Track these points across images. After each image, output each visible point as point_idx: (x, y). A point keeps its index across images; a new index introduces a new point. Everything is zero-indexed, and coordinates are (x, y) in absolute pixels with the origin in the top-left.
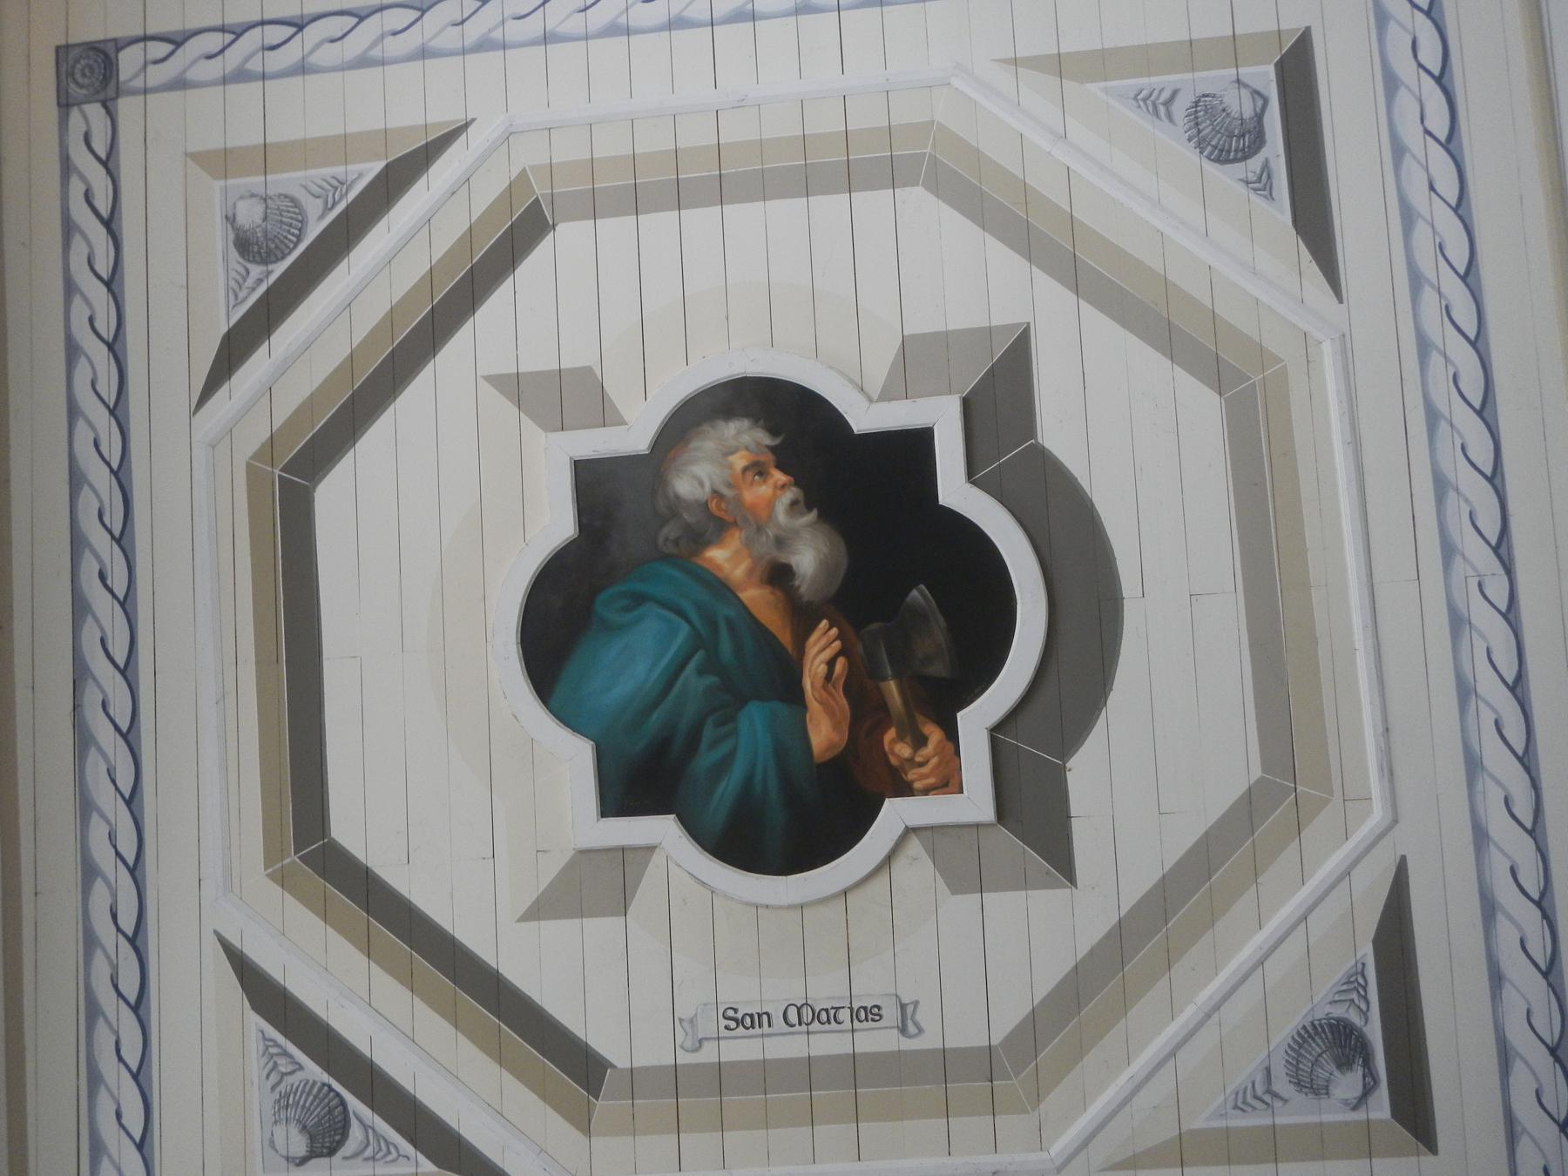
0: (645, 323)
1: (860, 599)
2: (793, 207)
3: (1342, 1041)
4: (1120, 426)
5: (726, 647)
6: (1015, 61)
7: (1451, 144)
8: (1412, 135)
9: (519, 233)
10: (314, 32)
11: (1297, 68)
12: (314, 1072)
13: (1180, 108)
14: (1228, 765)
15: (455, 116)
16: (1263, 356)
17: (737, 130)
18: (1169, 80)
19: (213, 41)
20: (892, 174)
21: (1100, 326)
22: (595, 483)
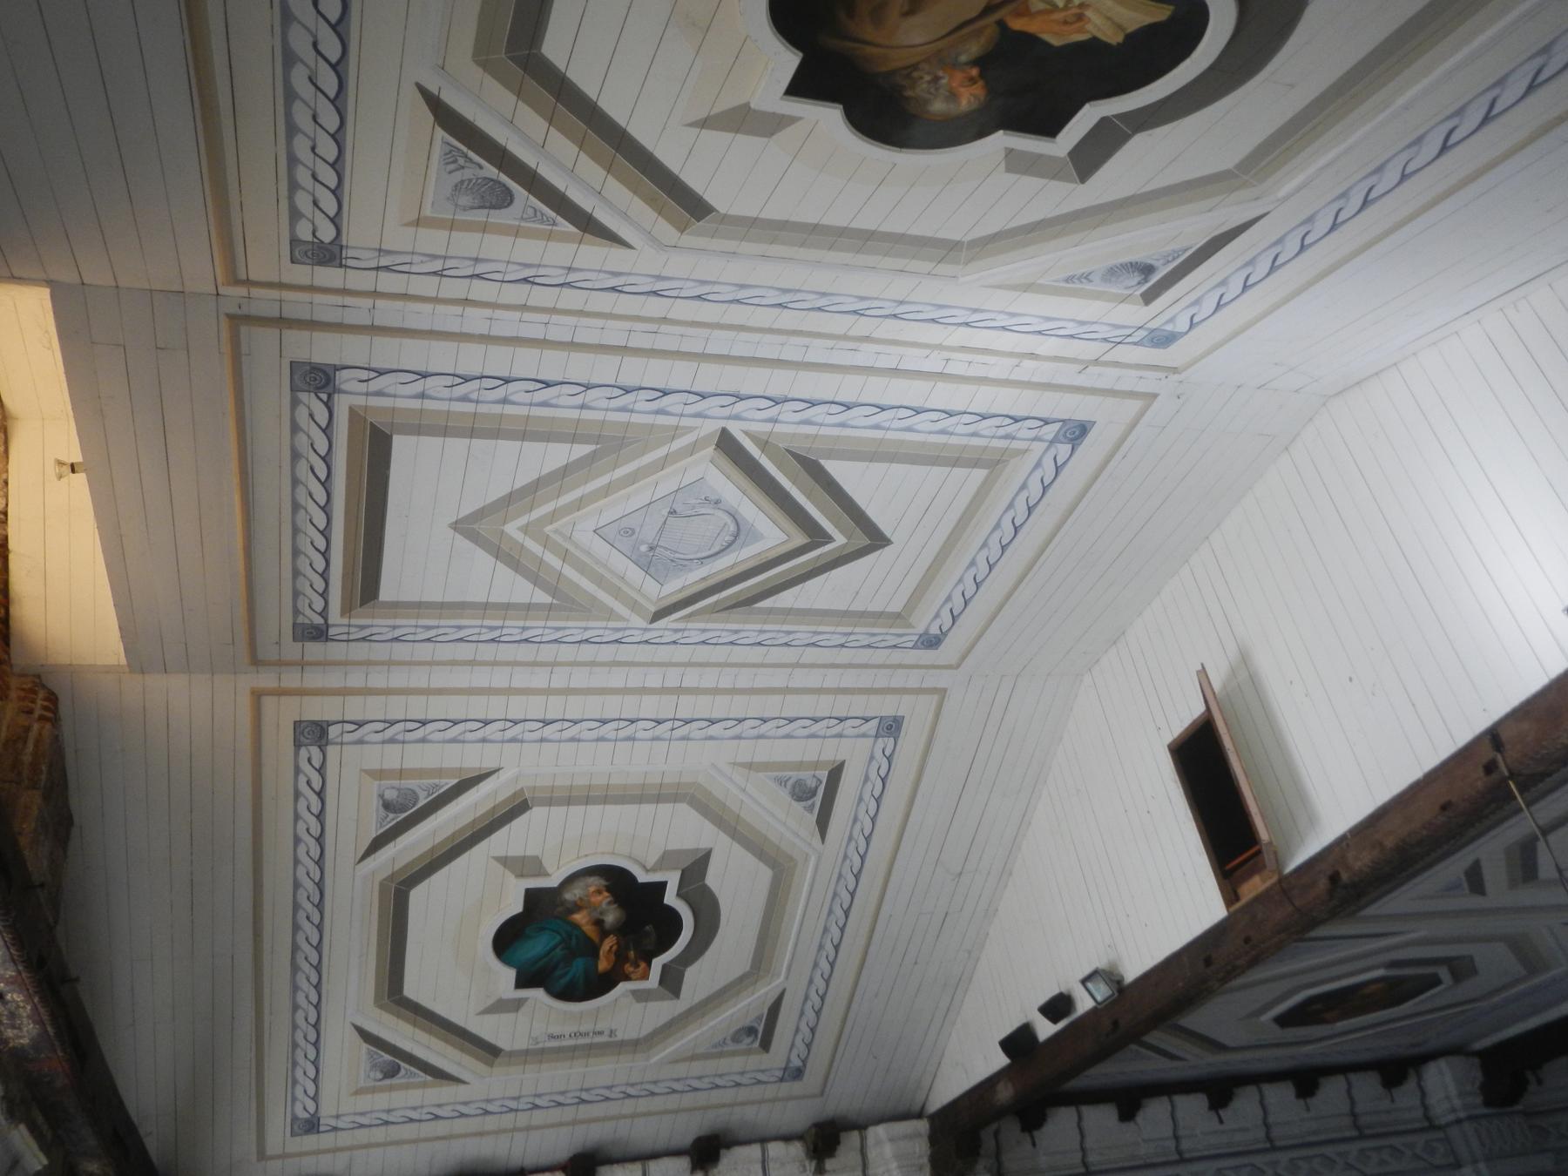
0: (562, 845)
1: (625, 930)
2: (634, 807)
3: (751, 1031)
4: (737, 883)
5: (574, 941)
7: (878, 801)
8: (867, 796)
9: (517, 808)
10: (430, 727)
11: (836, 773)
12: (388, 1057)
13: (790, 783)
14: (742, 965)
15: (494, 765)
16: (791, 859)
19: (380, 726)
20: (675, 798)
21: (737, 849)
22: (532, 897)
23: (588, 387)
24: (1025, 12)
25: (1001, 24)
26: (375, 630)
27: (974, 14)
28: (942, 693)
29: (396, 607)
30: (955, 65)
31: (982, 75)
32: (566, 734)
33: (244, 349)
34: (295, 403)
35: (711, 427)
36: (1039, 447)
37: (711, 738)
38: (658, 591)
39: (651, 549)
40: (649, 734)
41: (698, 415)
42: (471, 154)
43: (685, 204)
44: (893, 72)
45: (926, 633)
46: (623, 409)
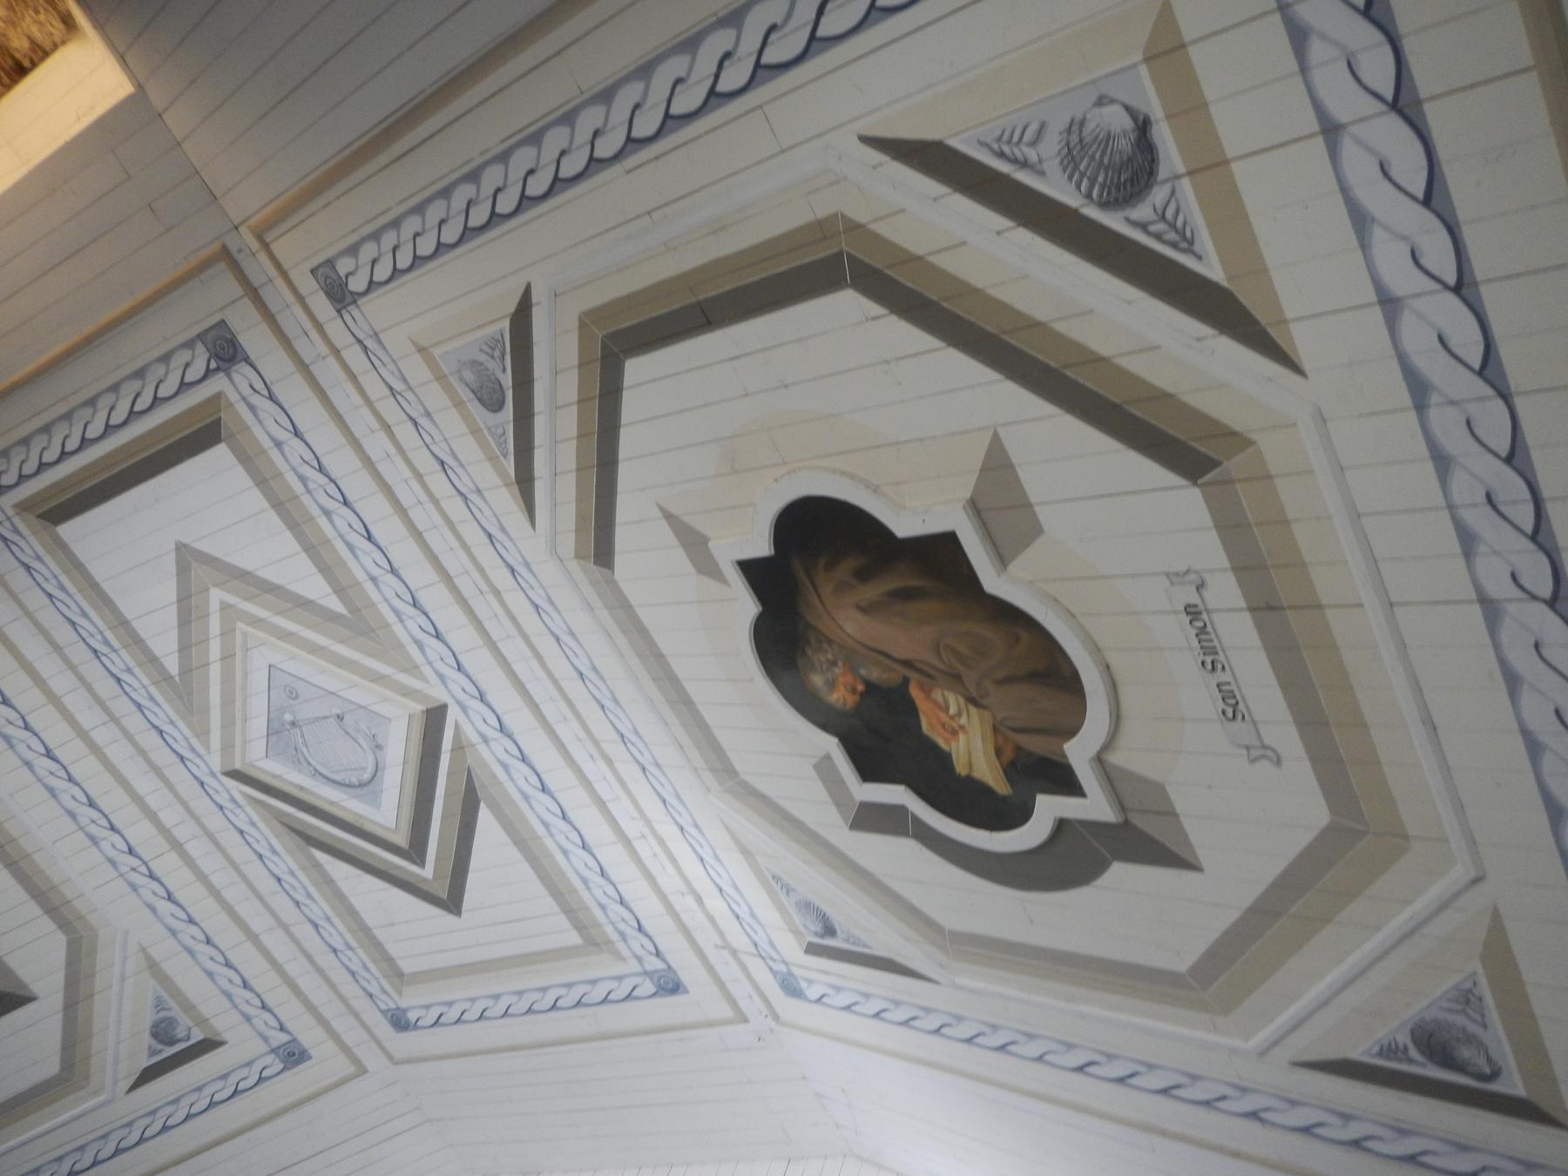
6: (143, 950)
7: (212, 1105)
8: (208, 1091)
13: (162, 1014)
16: (87, 1078)
17: (37, 858)
18: (171, 1003)
20: (64, 925)
23: (393, 571)
24: (927, 692)
25: (906, 681)
26: (22, 543)
27: (896, 655)
28: (361, 1070)
29: (61, 546)
30: (853, 669)
31: (862, 695)
32: (52, 781)
33: (203, 276)
34: (189, 344)
35: (439, 694)
36: (634, 966)
37: (153, 910)
39: (293, 724)
40: (112, 853)
41: (442, 677)
43: (600, 545)
45: (405, 1011)
46: (397, 613)
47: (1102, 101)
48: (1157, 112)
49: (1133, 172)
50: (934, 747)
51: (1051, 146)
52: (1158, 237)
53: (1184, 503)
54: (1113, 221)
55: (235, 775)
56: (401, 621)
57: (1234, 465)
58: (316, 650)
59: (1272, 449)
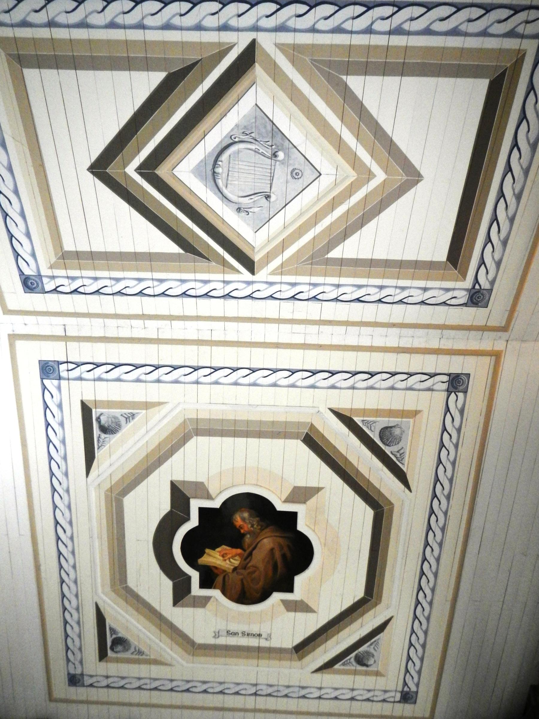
23: (336, 300)
24: (239, 555)
25: (244, 550)
27: (254, 552)
30: (249, 532)
31: (239, 531)
33: (507, 313)
34: (493, 283)
35: (262, 275)
38: (256, 97)
39: (275, 155)
41: (271, 284)
42: (394, 459)
43: (314, 442)
44: (267, 527)
46: (315, 285)
47: (375, 662)
48: (368, 669)
49: (360, 661)
50: (218, 547)
51: (372, 650)
52: (347, 661)
53: (289, 643)
54: (353, 655)
55: (248, 58)
56: (310, 284)
57: (295, 656)
58: (316, 218)
59: (297, 664)
